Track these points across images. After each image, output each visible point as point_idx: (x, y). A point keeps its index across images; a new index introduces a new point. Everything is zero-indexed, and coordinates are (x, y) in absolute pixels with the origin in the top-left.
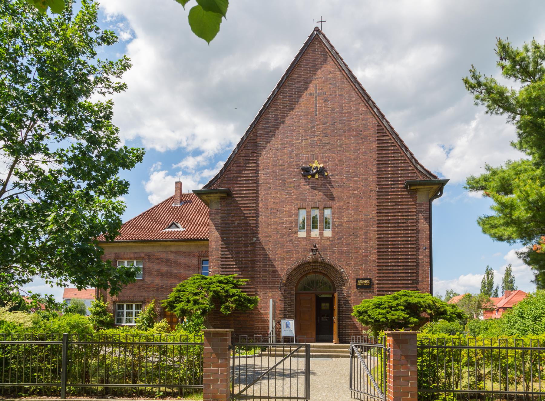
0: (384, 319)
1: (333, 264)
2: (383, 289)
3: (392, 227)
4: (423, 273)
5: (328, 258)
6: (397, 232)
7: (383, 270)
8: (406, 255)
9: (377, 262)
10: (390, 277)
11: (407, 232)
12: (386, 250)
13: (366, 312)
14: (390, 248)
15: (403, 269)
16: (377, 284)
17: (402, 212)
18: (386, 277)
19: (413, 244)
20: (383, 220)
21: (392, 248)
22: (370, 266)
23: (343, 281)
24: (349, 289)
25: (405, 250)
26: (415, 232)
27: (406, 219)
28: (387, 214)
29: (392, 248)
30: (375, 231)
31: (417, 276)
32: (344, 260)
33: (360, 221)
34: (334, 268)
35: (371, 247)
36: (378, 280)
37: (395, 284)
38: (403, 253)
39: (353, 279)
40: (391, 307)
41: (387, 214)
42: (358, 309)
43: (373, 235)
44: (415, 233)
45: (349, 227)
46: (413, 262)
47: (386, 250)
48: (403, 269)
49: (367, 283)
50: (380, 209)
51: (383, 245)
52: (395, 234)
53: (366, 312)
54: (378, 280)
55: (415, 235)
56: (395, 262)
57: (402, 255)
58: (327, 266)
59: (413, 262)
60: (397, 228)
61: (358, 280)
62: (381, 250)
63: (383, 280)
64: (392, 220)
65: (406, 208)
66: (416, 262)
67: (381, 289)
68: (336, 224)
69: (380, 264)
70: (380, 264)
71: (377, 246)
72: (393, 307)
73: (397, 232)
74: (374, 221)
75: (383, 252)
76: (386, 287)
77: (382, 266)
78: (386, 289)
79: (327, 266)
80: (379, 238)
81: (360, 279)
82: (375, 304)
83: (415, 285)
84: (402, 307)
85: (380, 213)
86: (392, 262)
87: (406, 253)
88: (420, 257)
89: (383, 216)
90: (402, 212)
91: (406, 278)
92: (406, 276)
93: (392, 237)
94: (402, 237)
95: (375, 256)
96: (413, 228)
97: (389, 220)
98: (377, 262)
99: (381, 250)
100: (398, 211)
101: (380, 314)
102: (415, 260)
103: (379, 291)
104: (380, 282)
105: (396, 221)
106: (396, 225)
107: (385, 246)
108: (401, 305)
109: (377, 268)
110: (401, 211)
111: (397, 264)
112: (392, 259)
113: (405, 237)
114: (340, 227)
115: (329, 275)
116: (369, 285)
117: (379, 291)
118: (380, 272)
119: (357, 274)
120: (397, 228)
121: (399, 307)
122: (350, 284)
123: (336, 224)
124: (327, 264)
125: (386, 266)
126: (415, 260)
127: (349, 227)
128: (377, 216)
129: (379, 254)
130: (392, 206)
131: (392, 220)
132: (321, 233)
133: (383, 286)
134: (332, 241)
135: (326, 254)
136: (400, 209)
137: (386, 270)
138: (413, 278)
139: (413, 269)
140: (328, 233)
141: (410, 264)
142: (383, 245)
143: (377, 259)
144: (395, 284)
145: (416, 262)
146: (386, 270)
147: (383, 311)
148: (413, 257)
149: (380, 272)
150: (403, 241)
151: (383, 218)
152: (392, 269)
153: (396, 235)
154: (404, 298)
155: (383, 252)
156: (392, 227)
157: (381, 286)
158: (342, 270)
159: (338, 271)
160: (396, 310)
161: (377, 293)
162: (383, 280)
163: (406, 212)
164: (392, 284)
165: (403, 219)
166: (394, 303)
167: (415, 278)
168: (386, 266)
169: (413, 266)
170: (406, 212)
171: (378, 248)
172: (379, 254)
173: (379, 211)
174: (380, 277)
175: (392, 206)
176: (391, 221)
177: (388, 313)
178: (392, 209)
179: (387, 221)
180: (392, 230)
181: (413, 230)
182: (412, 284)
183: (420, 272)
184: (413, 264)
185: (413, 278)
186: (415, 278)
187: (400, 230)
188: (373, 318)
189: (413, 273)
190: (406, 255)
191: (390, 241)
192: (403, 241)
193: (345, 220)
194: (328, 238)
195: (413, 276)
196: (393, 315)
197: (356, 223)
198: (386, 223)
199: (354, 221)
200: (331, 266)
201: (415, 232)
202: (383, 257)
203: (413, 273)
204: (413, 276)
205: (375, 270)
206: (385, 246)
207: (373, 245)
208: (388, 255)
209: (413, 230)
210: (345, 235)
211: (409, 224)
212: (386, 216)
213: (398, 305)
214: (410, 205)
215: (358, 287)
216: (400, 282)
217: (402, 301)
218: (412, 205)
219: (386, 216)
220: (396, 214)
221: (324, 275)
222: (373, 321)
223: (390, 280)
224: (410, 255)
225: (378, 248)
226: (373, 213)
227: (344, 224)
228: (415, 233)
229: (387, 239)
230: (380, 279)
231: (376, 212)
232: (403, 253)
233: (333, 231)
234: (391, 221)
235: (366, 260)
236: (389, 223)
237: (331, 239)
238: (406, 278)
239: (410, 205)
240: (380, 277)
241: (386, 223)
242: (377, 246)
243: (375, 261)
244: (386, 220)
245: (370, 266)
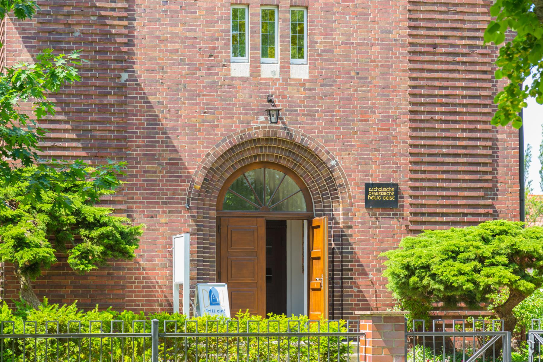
0: (469, 286)
1: (312, 145)
2: (425, 210)
3: (442, 62)
4: (507, 174)
5: (303, 129)
6: (451, 75)
7: (422, 163)
8: (471, 131)
9: (411, 146)
10: (438, 180)
11: (472, 76)
12: (428, 117)
13: (427, 267)
14: (436, 113)
15: (464, 164)
16: (411, 196)
17: (463, 29)
18: (430, 180)
19: (485, 106)
20: (421, 45)
21: (442, 113)
22: (395, 155)
23: (332, 188)
24: (349, 209)
25: (469, 118)
26: (489, 76)
27: (470, 46)
28: (431, 33)
29: (442, 113)
30: (404, 71)
31: (494, 181)
32: (338, 137)
33: (373, 45)
34: (314, 156)
35: (397, 108)
36: (411, 188)
37: (448, 197)
38: (465, 126)
39: (357, 184)
40: (481, 259)
41: (431, 33)
42: (407, 260)
43: (402, 81)
44: (490, 81)
45: (347, 58)
46: (485, 147)
47: (428, 117)
48: (464, 164)
49: (386, 194)
50: (415, 20)
51: (422, 104)
52: (447, 79)
53: (427, 267)
54: (411, 188)
55: (489, 85)
56: (448, 147)
57: (464, 130)
58: (296, 151)
59: (485, 147)
60: (451, 67)
61: (368, 186)
62: (418, 117)
63: (423, 189)
64: (442, 46)
65: (470, 21)
66: (491, 148)
67: (419, 210)
68: (320, 48)
69: (416, 151)
70: (416, 151)
71: (409, 107)
72: (486, 258)
73: (451, 75)
74: (403, 46)
75: (422, 121)
76: (429, 206)
77: (422, 154)
78: (430, 210)
79: (296, 151)
80: (415, 87)
81: (373, 185)
82: (445, 252)
83: (489, 202)
84: (504, 259)
85: (415, 28)
86: (442, 146)
87: (472, 126)
88: (499, 137)
89: (422, 36)
90: (463, 29)
91: (473, 185)
92: (471, 181)
93: (441, 88)
94: (463, 88)
95: (404, 130)
96: (485, 68)
97: (435, 46)
98: (411, 146)
99: (418, 117)
100: (454, 25)
101: (461, 273)
102: (489, 143)
103: (415, 214)
104: (417, 193)
105: (450, 50)
106: (450, 59)
107: (428, 108)
108: (500, 254)
109: (409, 158)
110: (459, 25)
111: (452, 151)
112: (443, 138)
113: (469, 88)
114: (328, 56)
115: (299, 172)
116: (392, 198)
117: (415, 214)
118: (417, 168)
119: (366, 173)
120: (451, 67)
121: (498, 258)
122: (350, 197)
123: (320, 48)
124: (299, 146)
125: (430, 155)
126: (489, 143)
127: (347, 58)
128: (410, 35)
129: (414, 125)
130: (441, 12)
131: (442, 46)
132: (285, 69)
133: (424, 202)
134: (310, 90)
135: (296, 122)
136: (457, 21)
137: (429, 163)
138: (485, 185)
139: (485, 164)
140: (300, 70)
141: (479, 152)
142: (422, 104)
143: (411, 137)
144: (448, 197)
145: (491, 148)
146: (429, 163)
147: (467, 268)
148: (486, 135)
149: (417, 168)
150: (464, 97)
151: (422, 41)
152: (443, 164)
153: (450, 84)
154: (508, 240)
155: (422, 121)
156: (442, 62)
157: (420, 201)
158: (333, 163)
159: (322, 164)
160: (492, 264)
161: (410, 218)
162: (423, 189)
163: (470, 30)
164: (443, 197)
165: (464, 46)
166: (486, 250)
167: (490, 185)
168: (430, 155)
169: (485, 156)
170: (470, 30)
171: (411, 112)
172: (414, 125)
173: (413, 24)
174: (417, 180)
175: (441, 12)
176: (439, 49)
177: (477, 271)
178: (441, 20)
179: (431, 49)
180: (442, 71)
181: (485, 72)
182: (484, 198)
183: (501, 170)
184: (485, 152)
185: (485, 185)
186: (490, 185)
187: (458, 71)
188: (441, 282)
189: (486, 173)
190: (471, 131)
191: (436, 96)
192: (464, 97)
193: (340, 39)
194: (301, 83)
195: (486, 181)
196: (488, 276)
197: (363, 48)
198: (428, 53)
199: (358, 44)
200: (306, 150)
201: (489, 76)
202: (423, 134)
203: (486, 173)
204: (486, 181)
205: (405, 161)
206: (428, 108)
207: (402, 102)
208: (434, 129)
209: (485, 72)
210: (338, 77)
211: (477, 59)
212: (428, 36)
213: (495, 253)
214: (478, 14)
215: (369, 203)
216: (459, 193)
217: (503, 245)
218: (483, 13)
219: (428, 36)
220: (449, 33)
221: (287, 171)
222: (442, 287)
223: (437, 188)
224: (478, 131)
225: (411, 112)
226: (400, 29)
227: (338, 51)
228: (490, 81)
229: (430, 92)
230: (417, 184)
231: (407, 24)
232: (465, 126)
233: (312, 66)
234: (439, 49)
235: (386, 139)
236: (434, 54)
237: (307, 85)
238: (473, 185)
239: (478, 14)
240: (417, 180)
241: (428, 53)
242: (409, 107)
243: (405, 142)
244: (429, 45)
245: (395, 155)
